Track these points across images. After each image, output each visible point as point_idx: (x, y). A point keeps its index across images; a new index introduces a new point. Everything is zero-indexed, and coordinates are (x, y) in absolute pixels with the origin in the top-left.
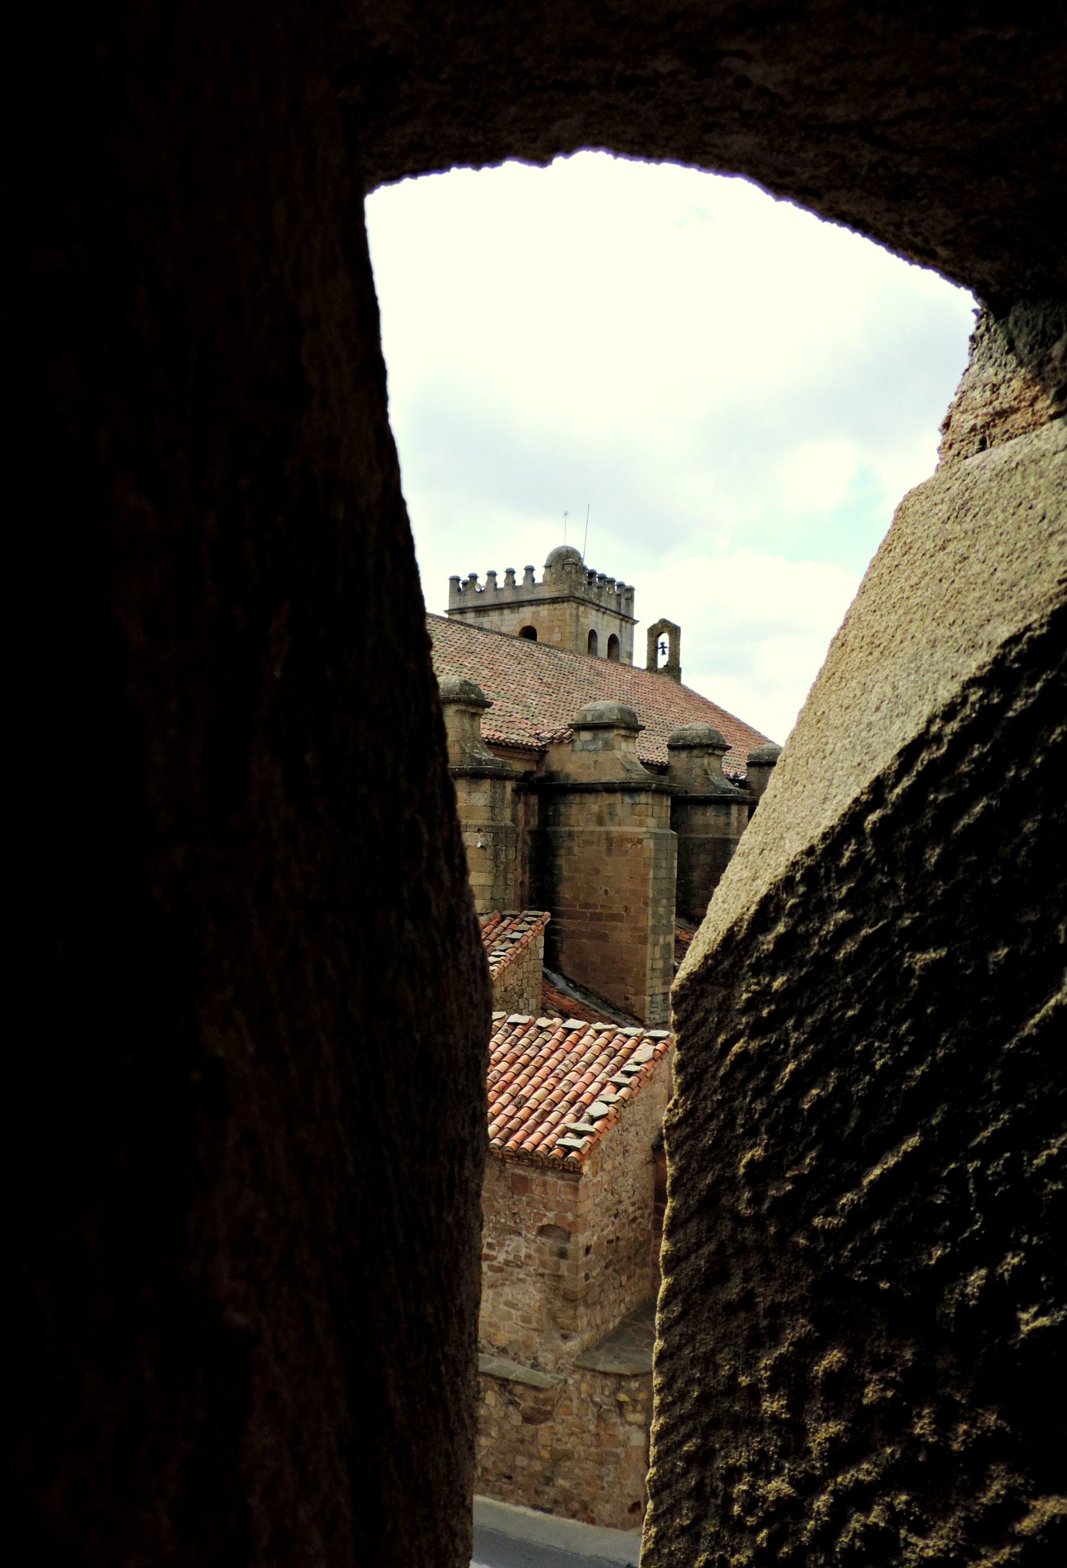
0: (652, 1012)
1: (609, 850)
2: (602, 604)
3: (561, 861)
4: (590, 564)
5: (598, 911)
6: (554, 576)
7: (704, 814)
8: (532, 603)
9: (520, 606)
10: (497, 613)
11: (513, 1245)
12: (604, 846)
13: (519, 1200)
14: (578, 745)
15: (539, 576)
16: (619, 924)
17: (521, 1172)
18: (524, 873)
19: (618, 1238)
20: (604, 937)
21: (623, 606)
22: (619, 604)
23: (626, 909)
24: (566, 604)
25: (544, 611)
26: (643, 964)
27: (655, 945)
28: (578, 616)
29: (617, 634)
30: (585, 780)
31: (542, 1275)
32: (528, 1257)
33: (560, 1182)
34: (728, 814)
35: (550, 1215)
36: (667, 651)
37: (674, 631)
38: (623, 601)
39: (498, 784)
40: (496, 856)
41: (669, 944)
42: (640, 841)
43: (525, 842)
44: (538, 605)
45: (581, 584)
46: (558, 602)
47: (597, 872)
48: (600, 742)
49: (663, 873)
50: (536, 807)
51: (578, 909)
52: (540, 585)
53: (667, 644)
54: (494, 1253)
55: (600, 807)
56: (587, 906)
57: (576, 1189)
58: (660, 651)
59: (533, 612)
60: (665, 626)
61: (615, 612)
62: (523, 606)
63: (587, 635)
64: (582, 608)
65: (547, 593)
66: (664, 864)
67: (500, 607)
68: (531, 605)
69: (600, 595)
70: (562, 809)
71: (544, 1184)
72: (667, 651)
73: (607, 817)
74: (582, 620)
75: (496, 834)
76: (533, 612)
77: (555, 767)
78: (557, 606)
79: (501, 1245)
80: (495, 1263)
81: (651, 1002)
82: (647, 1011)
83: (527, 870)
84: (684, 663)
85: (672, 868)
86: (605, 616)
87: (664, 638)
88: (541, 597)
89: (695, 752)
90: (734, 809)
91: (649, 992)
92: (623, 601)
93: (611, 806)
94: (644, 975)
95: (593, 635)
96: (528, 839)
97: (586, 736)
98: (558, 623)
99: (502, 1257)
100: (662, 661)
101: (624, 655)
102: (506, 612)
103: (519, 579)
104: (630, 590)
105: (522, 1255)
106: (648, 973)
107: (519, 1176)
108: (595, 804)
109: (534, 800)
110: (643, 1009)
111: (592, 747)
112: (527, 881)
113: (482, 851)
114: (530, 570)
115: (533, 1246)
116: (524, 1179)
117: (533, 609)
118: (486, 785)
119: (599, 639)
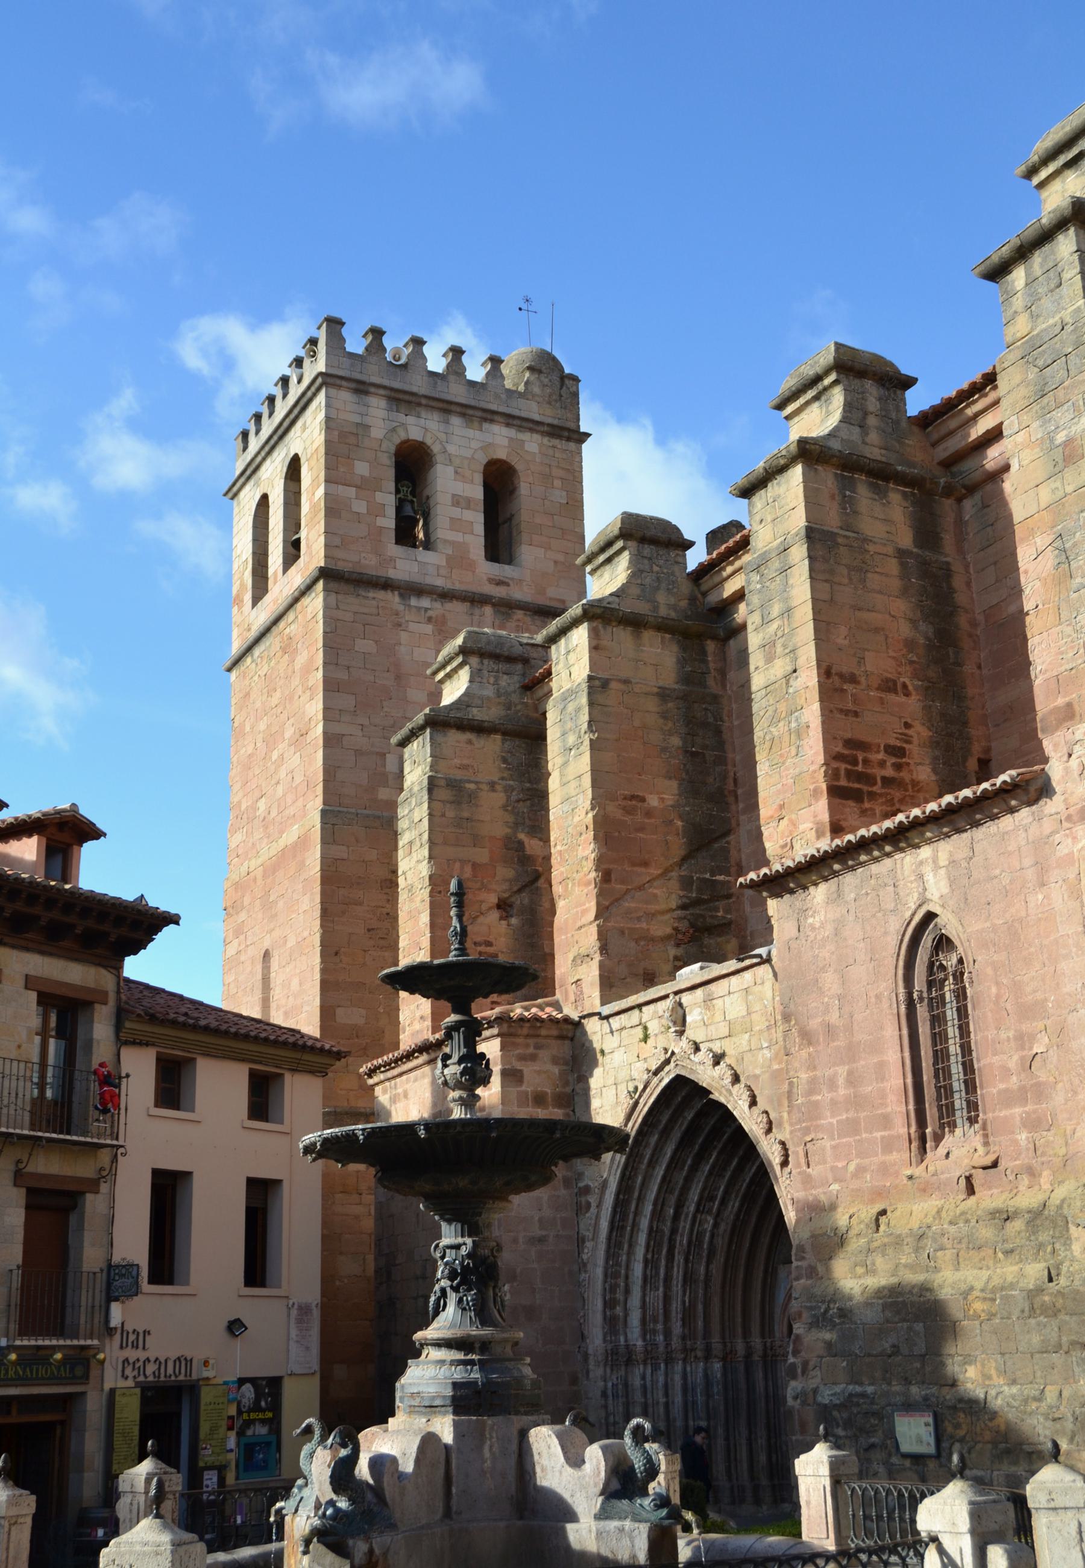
8: (510, 420)
9: (485, 420)
10: (436, 416)
44: (520, 428)
46: (560, 437)
59: (511, 439)
62: (492, 421)
68: (508, 425)
76: (511, 439)
78: (556, 442)
102: (456, 421)
117: (512, 432)
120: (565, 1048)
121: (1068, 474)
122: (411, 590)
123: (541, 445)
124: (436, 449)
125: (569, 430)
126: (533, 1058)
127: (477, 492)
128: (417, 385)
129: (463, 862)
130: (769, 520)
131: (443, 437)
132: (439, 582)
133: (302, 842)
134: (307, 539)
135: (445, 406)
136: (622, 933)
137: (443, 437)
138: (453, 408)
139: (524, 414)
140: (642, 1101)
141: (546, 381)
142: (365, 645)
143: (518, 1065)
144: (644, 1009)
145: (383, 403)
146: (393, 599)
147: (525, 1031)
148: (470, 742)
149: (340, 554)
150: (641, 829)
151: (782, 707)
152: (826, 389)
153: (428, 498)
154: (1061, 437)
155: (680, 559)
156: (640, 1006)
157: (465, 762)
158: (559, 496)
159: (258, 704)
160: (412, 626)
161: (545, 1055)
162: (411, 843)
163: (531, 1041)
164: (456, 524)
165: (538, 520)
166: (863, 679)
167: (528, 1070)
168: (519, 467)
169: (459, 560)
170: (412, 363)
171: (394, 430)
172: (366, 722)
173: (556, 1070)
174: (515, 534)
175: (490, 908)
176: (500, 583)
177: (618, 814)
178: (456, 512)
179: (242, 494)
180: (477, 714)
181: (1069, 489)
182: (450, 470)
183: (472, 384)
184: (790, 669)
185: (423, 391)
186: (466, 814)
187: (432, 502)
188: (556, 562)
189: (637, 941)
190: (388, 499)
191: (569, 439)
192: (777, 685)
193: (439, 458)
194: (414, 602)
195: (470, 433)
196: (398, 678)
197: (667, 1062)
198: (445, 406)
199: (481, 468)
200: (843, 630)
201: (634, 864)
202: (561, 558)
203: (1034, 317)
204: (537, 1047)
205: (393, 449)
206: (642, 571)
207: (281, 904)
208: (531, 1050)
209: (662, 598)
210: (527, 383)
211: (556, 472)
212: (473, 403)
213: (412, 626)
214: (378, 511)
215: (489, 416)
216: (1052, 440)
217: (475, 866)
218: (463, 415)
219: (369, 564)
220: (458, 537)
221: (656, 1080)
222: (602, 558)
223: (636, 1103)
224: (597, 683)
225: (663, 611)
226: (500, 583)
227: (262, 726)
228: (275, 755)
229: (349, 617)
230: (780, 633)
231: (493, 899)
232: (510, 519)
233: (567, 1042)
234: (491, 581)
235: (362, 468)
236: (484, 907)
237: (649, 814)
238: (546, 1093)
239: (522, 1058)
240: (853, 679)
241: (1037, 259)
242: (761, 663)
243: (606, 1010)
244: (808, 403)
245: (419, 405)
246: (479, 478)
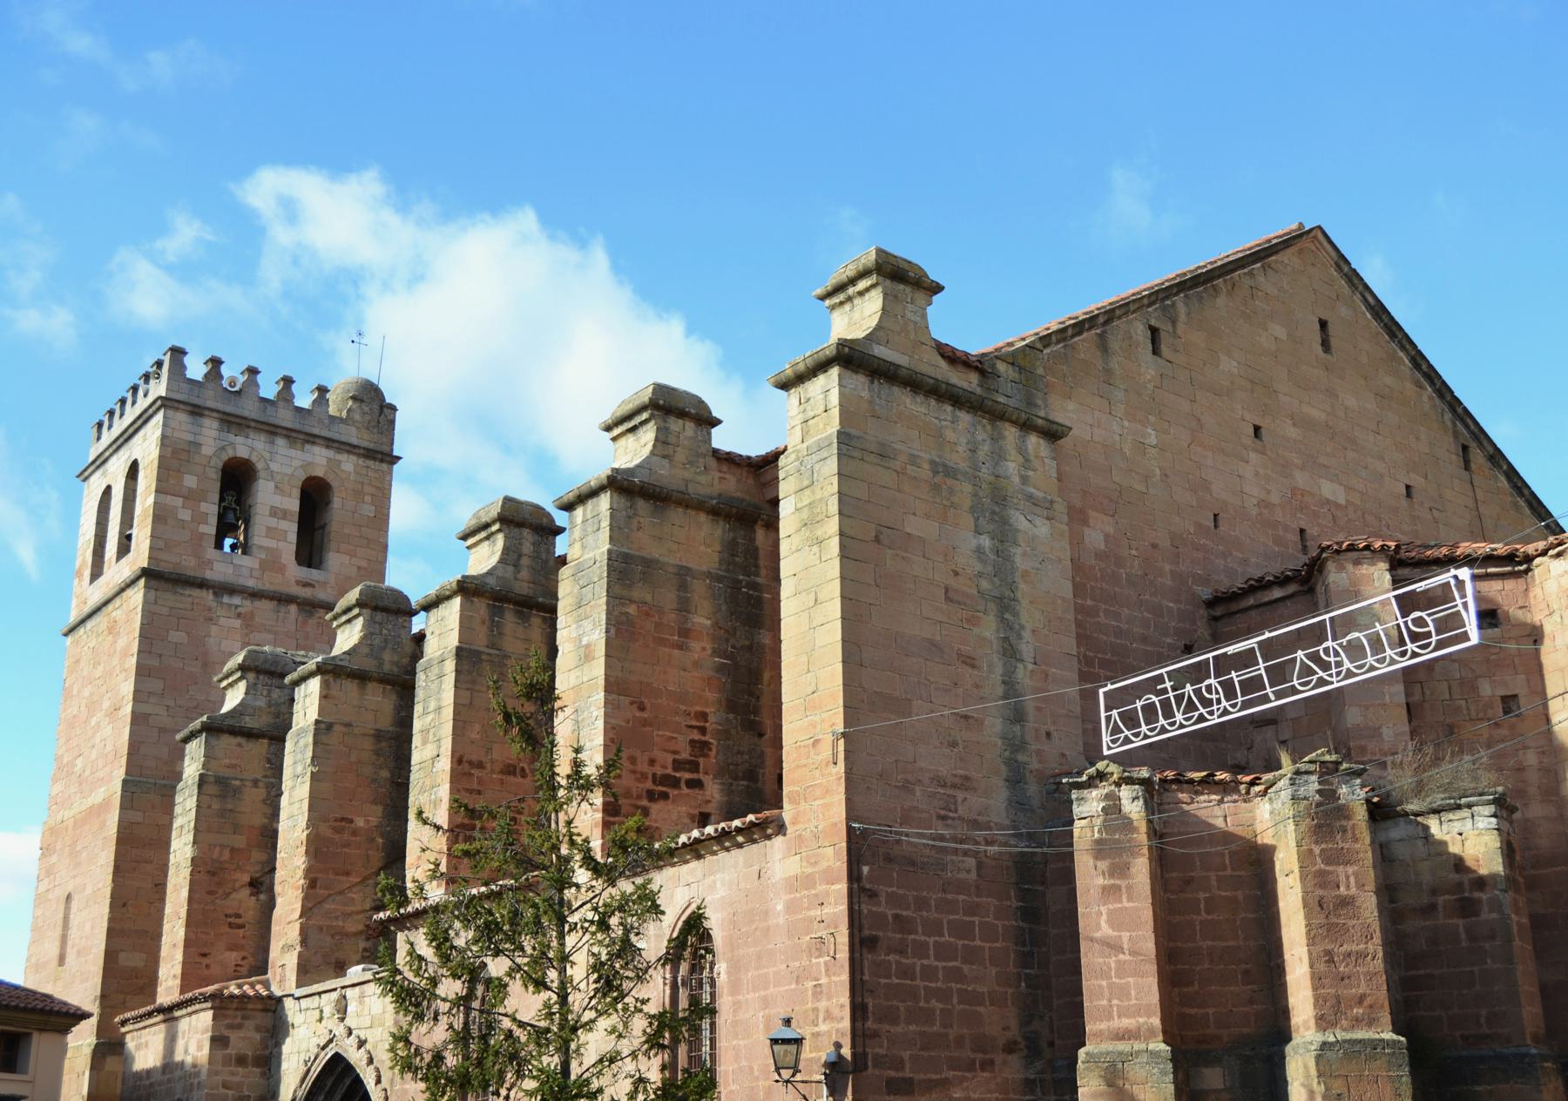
6: (368, 417)
8: (329, 443)
9: (308, 442)
10: (263, 437)
44: (339, 450)
46: (374, 459)
59: (329, 460)
62: (313, 443)
68: (328, 447)
76: (329, 460)
78: (370, 463)
98: (372, 490)
102: (280, 442)
117: (331, 453)
120: (267, 1020)
121: (586, 667)
122: (224, 589)
123: (356, 466)
124: (260, 466)
125: (382, 453)
126: (239, 1027)
127: (293, 504)
128: (249, 409)
129: (222, 846)
130: (437, 632)
131: (267, 455)
132: (251, 583)
133: (103, 807)
134: (137, 537)
135: (272, 429)
136: (321, 929)
137: (267, 455)
138: (279, 431)
139: (343, 439)
140: (313, 1069)
141: (366, 409)
142: (177, 636)
143: (226, 1033)
144: (323, 996)
145: (216, 424)
146: (208, 597)
147: (234, 1005)
148: (240, 745)
149: (163, 556)
150: (347, 845)
151: (428, 782)
152: (493, 534)
153: (250, 506)
154: (585, 641)
155: (406, 624)
156: (319, 994)
157: (234, 762)
158: (368, 510)
159: (85, 673)
160: (222, 621)
161: (250, 1024)
162: (182, 827)
163: (239, 1013)
164: (271, 532)
165: (347, 531)
166: (488, 766)
167: (234, 1037)
168: (334, 484)
169: (272, 564)
170: (246, 390)
171: (223, 448)
172: (171, 703)
173: (258, 1037)
174: (325, 540)
175: (243, 886)
176: (306, 585)
177: (328, 833)
178: (273, 522)
179: (93, 478)
180: (249, 722)
181: (585, 680)
182: (271, 485)
183: (299, 410)
184: (435, 753)
185: (253, 415)
186: (229, 806)
187: (253, 511)
188: (359, 568)
189: (332, 936)
190: (211, 509)
191: (382, 461)
192: (426, 764)
193: (262, 474)
194: (226, 599)
195: (293, 453)
196: (205, 665)
197: (331, 1041)
198: (272, 429)
199: (300, 484)
200: (477, 727)
201: (337, 874)
202: (364, 564)
203: (584, 547)
204: (244, 1018)
205: (220, 465)
206: (372, 634)
207: (84, 855)
208: (238, 1020)
209: (387, 656)
210: (349, 411)
211: (367, 489)
212: (297, 426)
213: (222, 621)
214: (201, 518)
215: (311, 439)
216: (580, 641)
217: (233, 850)
218: (288, 437)
219: (188, 564)
220: (271, 544)
221: (323, 1053)
222: (344, 618)
223: (309, 1070)
224: (323, 726)
225: (387, 667)
226: (306, 585)
227: (86, 693)
228: (93, 722)
229: (165, 611)
230: (432, 724)
231: (246, 878)
232: (323, 527)
233: (270, 1014)
234: (298, 583)
235: (190, 481)
236: (237, 885)
237: (355, 833)
238: (248, 1055)
239: (231, 1027)
240: (480, 765)
241: (590, 504)
242: (419, 744)
243: (298, 993)
244: (481, 541)
245: (249, 427)
246: (297, 493)
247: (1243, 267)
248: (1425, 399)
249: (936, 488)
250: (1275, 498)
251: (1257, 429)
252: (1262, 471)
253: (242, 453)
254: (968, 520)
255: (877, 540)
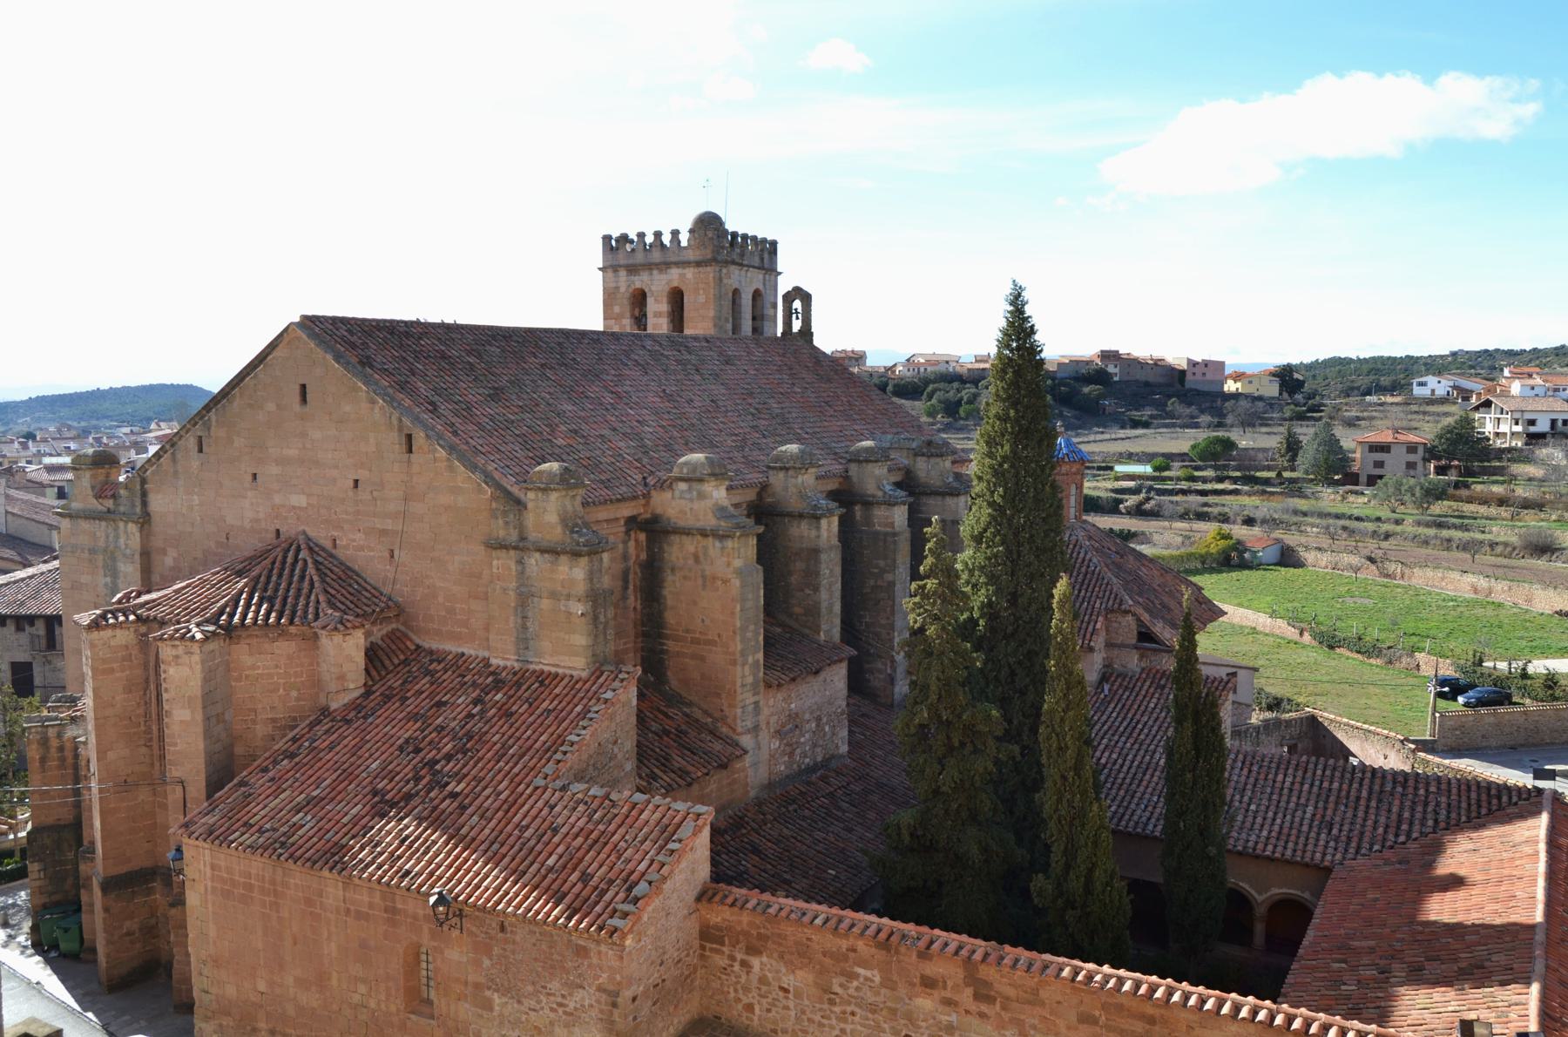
0: (743, 721)
1: (704, 586)
2: (745, 262)
3: (666, 592)
4: (730, 226)
5: (697, 636)
7: (799, 527)
8: (678, 264)
11: (580, 996)
12: (700, 581)
13: (582, 964)
14: (677, 493)
15: (684, 239)
16: (714, 648)
17: (582, 943)
18: (636, 600)
19: (664, 981)
20: (702, 659)
21: (766, 261)
22: (762, 259)
23: (719, 636)
24: (709, 269)
25: (690, 273)
26: (734, 683)
27: (743, 665)
28: (721, 279)
29: (761, 287)
30: (681, 523)
31: (601, 1019)
32: (591, 1006)
33: (610, 952)
34: (818, 528)
35: (605, 975)
36: (800, 316)
37: (806, 298)
38: (766, 256)
39: (595, 558)
40: (595, 618)
41: (758, 661)
42: (729, 581)
43: (635, 573)
45: (723, 248)
47: (695, 603)
48: (695, 493)
49: (749, 604)
50: (644, 544)
51: (681, 633)
52: (685, 248)
53: (800, 310)
54: (566, 1002)
55: (696, 547)
56: (687, 631)
57: (621, 958)
58: (794, 316)
59: (680, 275)
60: (799, 293)
61: (759, 268)
63: (731, 294)
64: (724, 271)
65: (691, 256)
66: (750, 596)
67: (650, 267)
69: (742, 255)
70: (666, 547)
71: (599, 953)
72: (800, 316)
73: (702, 559)
74: (725, 281)
75: (595, 602)
76: (680, 275)
77: (659, 511)
78: (701, 269)
79: (571, 995)
80: (567, 1009)
81: (743, 712)
82: (739, 721)
83: (639, 597)
84: (816, 327)
85: (758, 597)
86: (749, 274)
87: (797, 304)
88: (685, 259)
89: (791, 472)
90: (824, 522)
91: (742, 704)
92: (766, 256)
93: (705, 548)
94: (735, 692)
95: (736, 292)
96: (638, 571)
97: (683, 486)
99: (572, 1005)
100: (797, 325)
101: (769, 306)
102: (655, 272)
103: (666, 239)
104: (774, 244)
105: (586, 1004)
106: (739, 690)
107: (581, 945)
108: (690, 545)
109: (642, 537)
110: (735, 719)
111: (688, 496)
112: (639, 607)
113: (583, 619)
114: (675, 233)
115: (594, 998)
116: (584, 948)
117: (680, 271)
118: (584, 561)
119: (743, 296)
123: (694, 274)
168: (684, 289)
247: (248, 374)
248: (377, 410)
249: (90, 561)
250: (261, 515)
251: (255, 476)
252: (254, 501)
253: (638, 285)
254: (101, 572)
255: (72, 588)
